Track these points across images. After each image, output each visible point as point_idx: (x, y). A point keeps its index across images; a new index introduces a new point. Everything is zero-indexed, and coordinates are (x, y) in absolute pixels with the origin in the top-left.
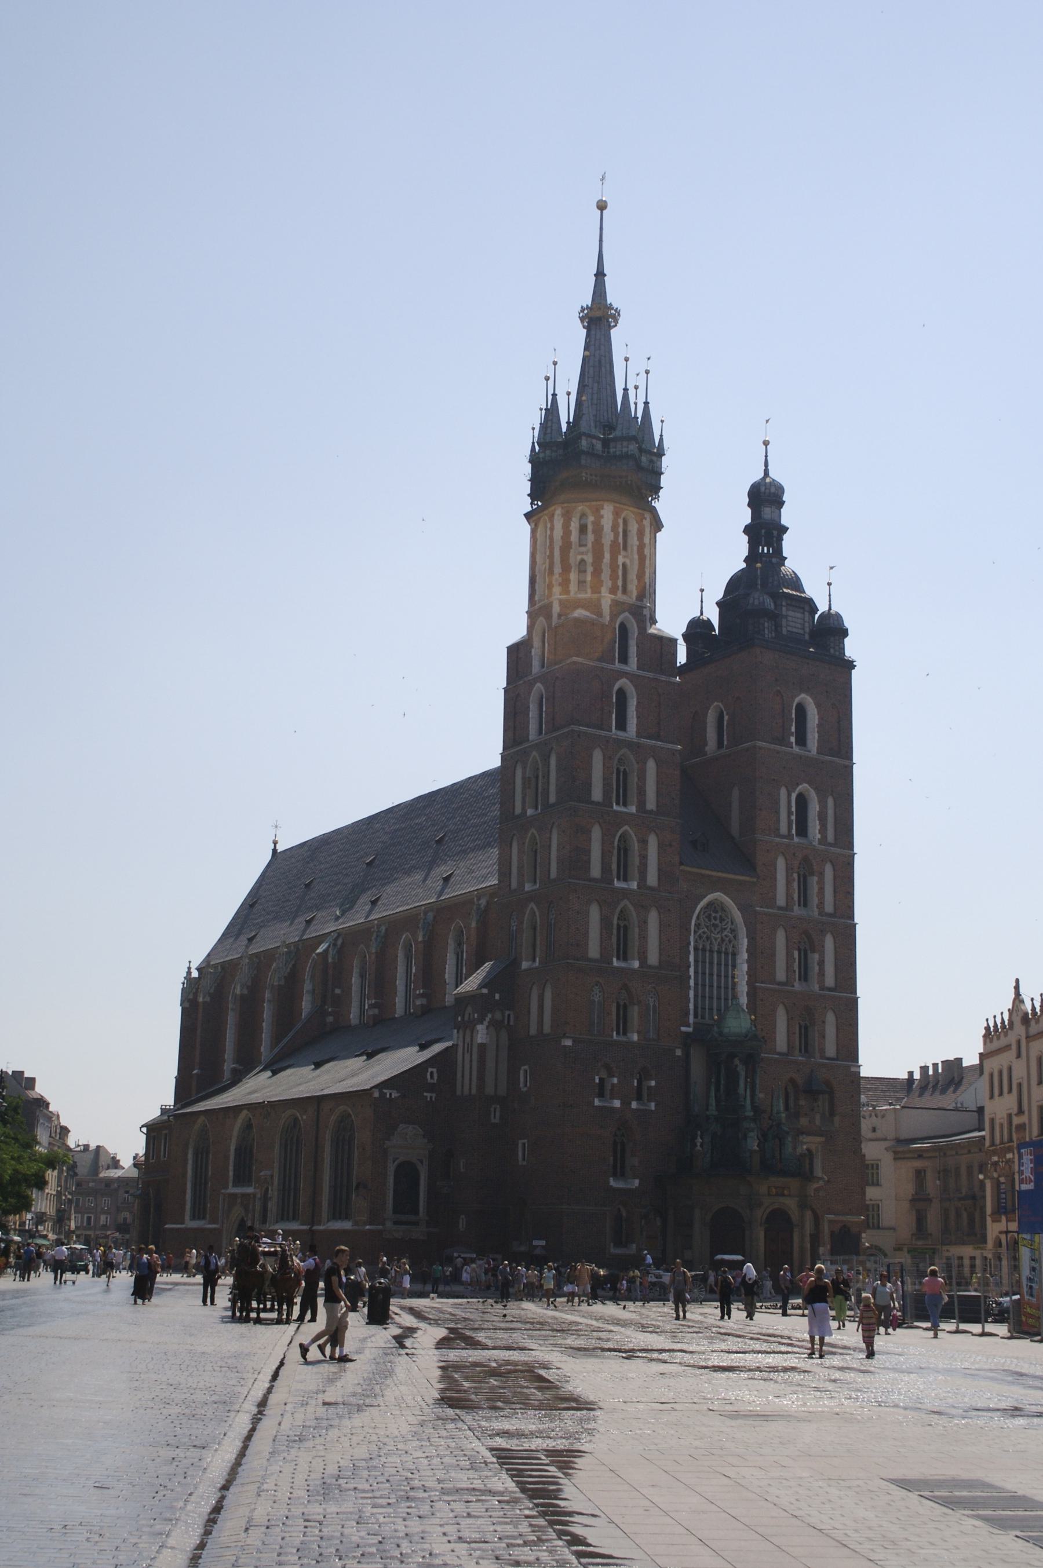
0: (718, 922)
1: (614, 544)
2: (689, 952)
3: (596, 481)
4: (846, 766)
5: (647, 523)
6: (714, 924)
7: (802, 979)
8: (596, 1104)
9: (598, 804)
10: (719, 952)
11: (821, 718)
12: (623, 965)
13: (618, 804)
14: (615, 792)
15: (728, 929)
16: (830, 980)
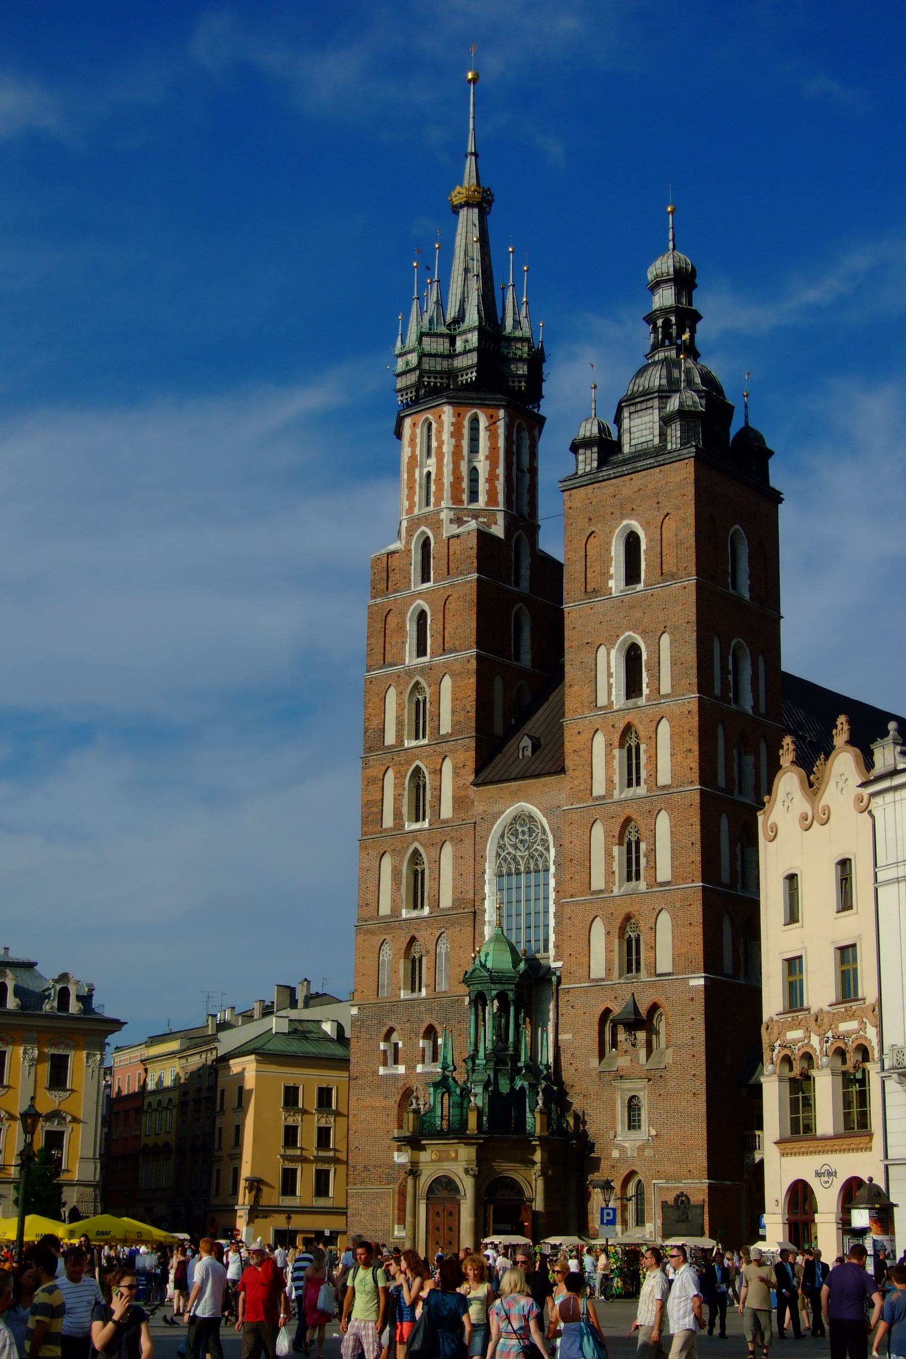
0: (526, 837)
1: (413, 457)
2: (485, 882)
3: (411, 398)
4: (685, 588)
5: (447, 412)
6: (522, 841)
7: (634, 879)
8: (380, 1074)
9: (389, 747)
10: (528, 872)
11: (650, 540)
12: (415, 914)
13: (417, 738)
14: (406, 729)
15: (539, 840)
16: (664, 872)
